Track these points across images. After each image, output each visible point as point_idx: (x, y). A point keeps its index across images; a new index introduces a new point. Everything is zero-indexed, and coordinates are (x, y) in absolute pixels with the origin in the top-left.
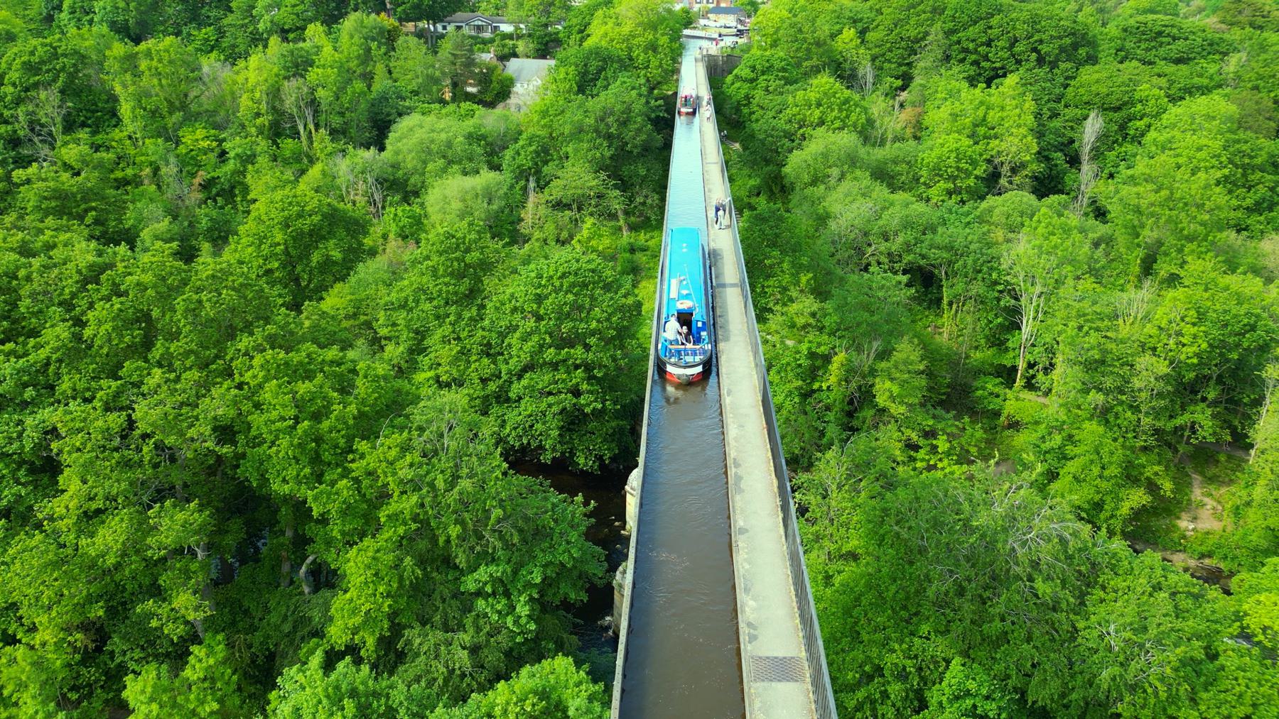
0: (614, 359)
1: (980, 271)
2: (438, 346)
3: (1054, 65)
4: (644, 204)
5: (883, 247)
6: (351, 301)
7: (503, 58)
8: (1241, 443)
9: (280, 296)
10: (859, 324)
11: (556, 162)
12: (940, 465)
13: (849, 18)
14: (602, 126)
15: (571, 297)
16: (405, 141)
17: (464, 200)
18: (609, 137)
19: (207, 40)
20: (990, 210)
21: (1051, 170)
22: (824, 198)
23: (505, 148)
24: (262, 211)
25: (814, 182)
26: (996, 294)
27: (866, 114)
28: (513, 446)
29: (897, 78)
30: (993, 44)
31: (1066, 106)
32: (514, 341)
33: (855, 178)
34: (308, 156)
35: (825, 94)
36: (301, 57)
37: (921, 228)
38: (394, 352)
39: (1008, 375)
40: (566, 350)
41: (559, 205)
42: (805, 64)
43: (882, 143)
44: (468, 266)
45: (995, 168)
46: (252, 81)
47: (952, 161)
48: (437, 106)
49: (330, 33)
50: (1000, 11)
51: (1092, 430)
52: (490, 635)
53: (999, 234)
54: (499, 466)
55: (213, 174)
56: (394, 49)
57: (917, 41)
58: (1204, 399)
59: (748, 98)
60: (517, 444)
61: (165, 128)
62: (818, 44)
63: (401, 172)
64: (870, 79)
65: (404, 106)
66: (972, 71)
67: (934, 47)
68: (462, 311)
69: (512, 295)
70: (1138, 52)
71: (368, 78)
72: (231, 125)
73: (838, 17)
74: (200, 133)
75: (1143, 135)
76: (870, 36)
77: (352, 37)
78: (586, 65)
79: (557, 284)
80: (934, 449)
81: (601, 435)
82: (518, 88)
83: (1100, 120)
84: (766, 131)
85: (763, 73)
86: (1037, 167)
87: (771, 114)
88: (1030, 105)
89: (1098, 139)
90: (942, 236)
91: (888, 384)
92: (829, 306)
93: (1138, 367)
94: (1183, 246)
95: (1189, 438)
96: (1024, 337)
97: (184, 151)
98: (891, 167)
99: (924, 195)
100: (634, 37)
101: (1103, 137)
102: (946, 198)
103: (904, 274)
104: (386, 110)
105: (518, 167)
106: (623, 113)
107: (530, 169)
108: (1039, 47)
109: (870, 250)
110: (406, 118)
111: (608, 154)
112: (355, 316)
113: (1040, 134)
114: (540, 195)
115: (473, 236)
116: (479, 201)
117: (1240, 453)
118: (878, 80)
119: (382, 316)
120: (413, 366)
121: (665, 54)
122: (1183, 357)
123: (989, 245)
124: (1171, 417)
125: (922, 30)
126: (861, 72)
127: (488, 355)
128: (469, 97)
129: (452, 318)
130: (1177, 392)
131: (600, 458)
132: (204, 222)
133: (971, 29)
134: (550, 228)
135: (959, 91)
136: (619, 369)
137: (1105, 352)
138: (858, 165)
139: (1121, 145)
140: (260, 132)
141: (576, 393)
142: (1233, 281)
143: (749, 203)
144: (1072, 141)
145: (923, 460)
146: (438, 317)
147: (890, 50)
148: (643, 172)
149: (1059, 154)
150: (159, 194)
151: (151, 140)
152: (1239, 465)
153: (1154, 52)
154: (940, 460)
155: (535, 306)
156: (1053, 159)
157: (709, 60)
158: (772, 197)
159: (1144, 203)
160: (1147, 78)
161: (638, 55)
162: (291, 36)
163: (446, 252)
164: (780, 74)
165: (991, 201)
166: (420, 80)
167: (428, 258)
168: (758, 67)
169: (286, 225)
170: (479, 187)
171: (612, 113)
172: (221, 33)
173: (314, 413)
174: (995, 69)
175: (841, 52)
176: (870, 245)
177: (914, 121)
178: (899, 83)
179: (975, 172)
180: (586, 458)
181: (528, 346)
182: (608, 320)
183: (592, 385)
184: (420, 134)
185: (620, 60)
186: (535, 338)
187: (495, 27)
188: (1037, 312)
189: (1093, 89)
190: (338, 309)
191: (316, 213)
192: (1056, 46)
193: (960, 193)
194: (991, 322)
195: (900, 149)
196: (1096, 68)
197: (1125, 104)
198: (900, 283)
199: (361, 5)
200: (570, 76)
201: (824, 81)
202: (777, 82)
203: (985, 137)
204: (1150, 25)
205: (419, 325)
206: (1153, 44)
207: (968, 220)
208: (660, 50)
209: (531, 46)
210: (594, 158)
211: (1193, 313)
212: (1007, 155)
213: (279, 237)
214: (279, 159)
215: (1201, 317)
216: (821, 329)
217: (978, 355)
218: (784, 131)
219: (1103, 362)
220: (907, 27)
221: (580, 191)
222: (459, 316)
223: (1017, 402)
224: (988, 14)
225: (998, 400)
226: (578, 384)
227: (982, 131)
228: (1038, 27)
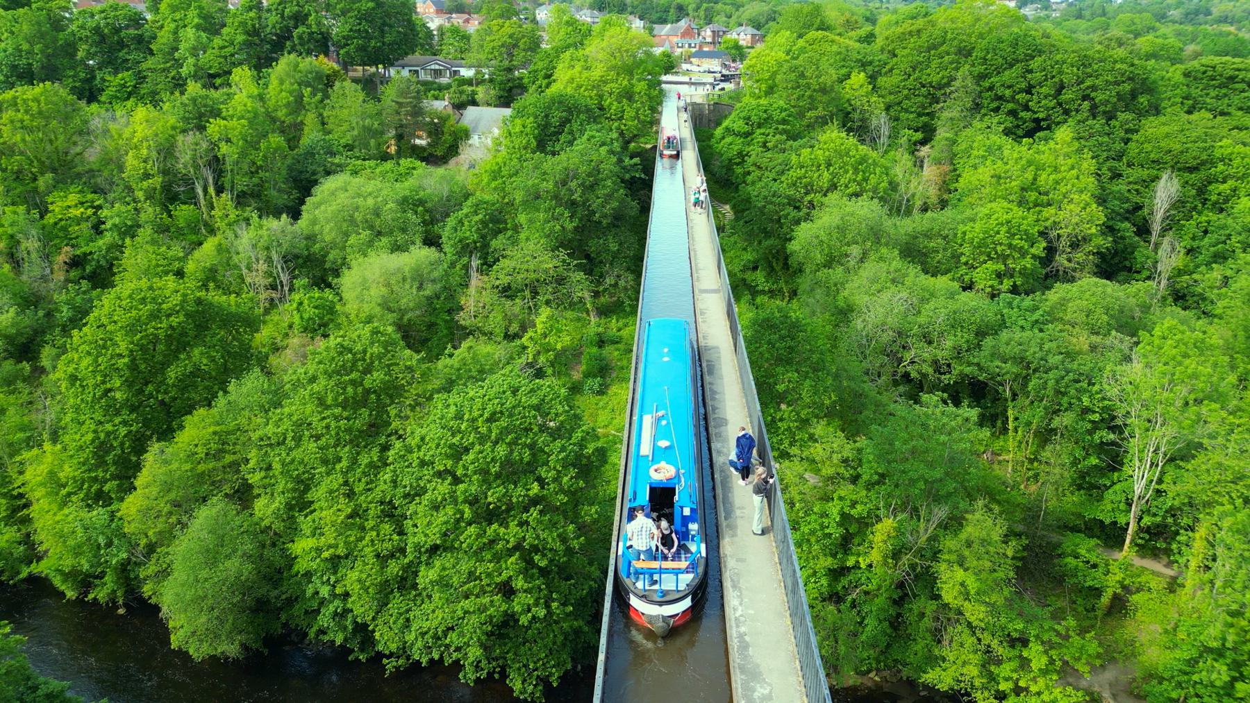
0: (563, 539)
1: (1064, 394)
2: (323, 504)
3: (1110, 116)
4: (616, 285)
5: (927, 353)
6: (215, 433)
7: (459, 107)
9: (125, 423)
10: (912, 482)
11: (509, 233)
12: (1033, 689)
13: (858, 61)
15: (502, 450)
16: (323, 207)
17: (388, 285)
19: (124, 86)
20: (1063, 303)
22: (842, 284)
23: (448, 215)
24: (106, 310)
25: (829, 263)
26: (1089, 426)
27: (887, 174)
28: (418, 663)
29: (916, 131)
30: (1034, 91)
31: (1129, 165)
32: (420, 509)
33: (881, 258)
34: (206, 225)
36: (205, 106)
37: (974, 327)
38: (266, 508)
40: (495, 526)
41: (507, 292)
42: (809, 114)
43: (908, 212)
44: (368, 392)
46: (139, 135)
47: (1002, 237)
48: (372, 163)
49: (260, 78)
50: (1040, 52)
53: (1082, 340)
55: (85, 249)
56: (328, 97)
57: (940, 87)
59: (742, 156)
60: (424, 661)
61: (35, 190)
62: (823, 90)
63: (317, 246)
64: (885, 131)
65: (333, 164)
66: (1009, 122)
67: (961, 93)
68: (358, 454)
70: (1208, 100)
71: (292, 133)
72: (115, 188)
73: (844, 60)
74: (73, 198)
75: (1226, 201)
76: (882, 81)
77: (282, 82)
78: (547, 116)
80: (1024, 664)
81: (545, 646)
82: (475, 140)
83: (1176, 181)
84: (765, 198)
85: (759, 126)
86: (1105, 243)
87: (772, 175)
88: (1089, 164)
89: (1173, 206)
90: (1008, 341)
91: (960, 574)
92: (862, 441)
97: (52, 221)
98: (923, 243)
99: (967, 278)
100: (605, 82)
101: (1179, 204)
102: (995, 283)
104: (311, 168)
105: (460, 241)
106: (589, 175)
107: (475, 242)
108: (1093, 95)
109: (908, 356)
110: (331, 178)
111: (570, 226)
112: (218, 455)
113: (1102, 200)
114: (486, 278)
115: (376, 349)
116: (407, 286)
118: (894, 136)
119: (253, 455)
120: (293, 530)
121: (642, 103)
123: (1070, 355)
125: (946, 73)
126: (874, 122)
127: (391, 516)
128: (417, 153)
131: (544, 681)
132: (65, 310)
133: (1007, 73)
134: (495, 321)
135: (1000, 148)
136: (569, 551)
138: (883, 241)
139: (1200, 213)
140: (149, 197)
141: (507, 591)
143: (744, 280)
144: (1139, 207)
145: (1007, 679)
146: (325, 462)
147: (907, 98)
148: (614, 247)
149: (1127, 225)
150: (12, 275)
151: (11, 208)
153: (1226, 101)
154: (1034, 679)
155: (449, 463)
156: (1119, 230)
157: (693, 109)
158: (771, 272)
160: (1224, 132)
161: (611, 104)
162: (218, 81)
163: (338, 373)
164: (781, 127)
165: (1059, 292)
166: (356, 133)
167: (313, 379)
168: (754, 118)
169: (131, 329)
170: (407, 269)
171: (575, 177)
172: (141, 78)
174: (1037, 121)
175: (848, 100)
177: (940, 182)
179: (1033, 251)
180: (524, 681)
181: (440, 518)
182: (555, 480)
184: (343, 198)
185: (588, 110)
186: (450, 510)
187: (455, 72)
189: (1162, 145)
190: (196, 446)
191: (178, 312)
192: (1114, 93)
193: (1012, 276)
195: (934, 219)
196: (1162, 119)
197: (1203, 163)
198: (967, 420)
199: (298, 47)
200: (528, 130)
201: (833, 136)
202: (778, 136)
203: (1036, 205)
204: (1219, 68)
205: (301, 469)
206: (1224, 91)
207: (1036, 316)
208: (637, 97)
210: (552, 230)
212: (1066, 227)
213: (123, 346)
214: (173, 230)
216: (855, 479)
218: (788, 197)
220: (928, 71)
221: (533, 276)
222: (354, 462)
224: (1026, 55)
225: (1099, 573)
227: (1032, 196)
228: (1089, 70)
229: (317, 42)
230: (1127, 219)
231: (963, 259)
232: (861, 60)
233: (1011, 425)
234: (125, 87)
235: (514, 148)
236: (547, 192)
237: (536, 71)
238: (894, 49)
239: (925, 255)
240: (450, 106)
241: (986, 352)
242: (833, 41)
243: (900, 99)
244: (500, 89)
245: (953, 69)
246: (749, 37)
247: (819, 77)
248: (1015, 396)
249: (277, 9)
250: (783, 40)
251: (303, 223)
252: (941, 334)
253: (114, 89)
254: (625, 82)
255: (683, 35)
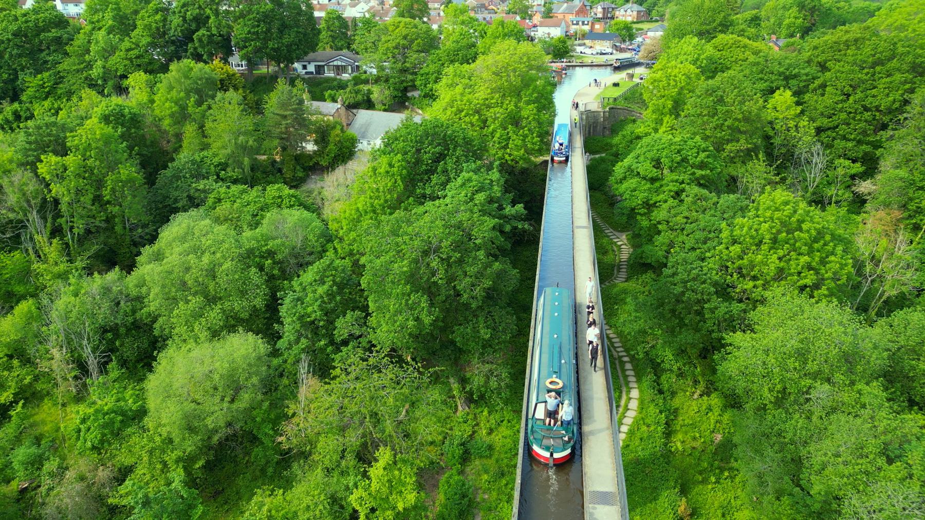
18: (431, 291)
29: (854, 161)
35: (783, 224)
42: (728, 147)
63: (145, 310)
73: (761, 72)
77: (171, 88)
78: (418, 151)
84: (685, 282)
100: (489, 107)
138: (859, 368)
157: (587, 117)
161: (494, 131)
164: (699, 173)
166: (229, 151)
175: (771, 123)
178: (858, 168)
208: (524, 123)
209: (387, 92)
220: (874, 92)
229: (218, 43)
232: (783, 73)
234: (44, 87)
235: (378, 190)
237: (427, 74)
238: (826, 61)
240: (343, 109)
242: (745, 46)
243: (836, 123)
244: (395, 89)
245: (906, 91)
246: (635, 13)
247: (742, 103)
249: (180, 12)
250: (690, 48)
251: (132, 280)
253: (32, 90)
254: (511, 107)
255: (578, 13)
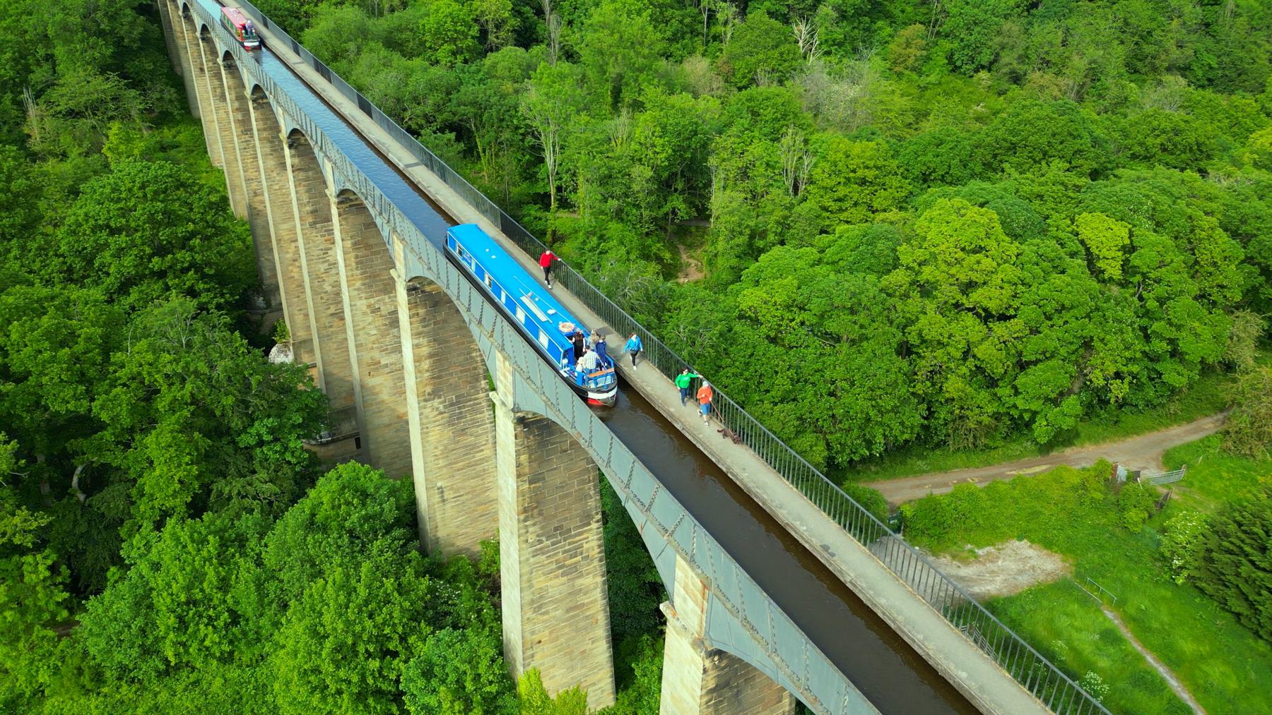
1: (502, 120)
4: (161, 99)
5: (419, 110)
8: (703, 214)
14: (89, 24)
18: (101, 34)
20: (494, 66)
21: (524, 22)
22: (349, 72)
26: (521, 137)
39: (543, 200)
43: (381, 14)
44: (17, 195)
45: (482, 26)
47: (449, 25)
51: (614, 227)
52: (276, 471)
53: (508, 87)
54: (242, 345)
58: (676, 190)
69: (86, 215)
79: (140, 194)
86: (515, 22)
93: (633, 175)
94: (637, 76)
95: (673, 219)
96: (550, 168)
99: (433, 58)
102: (452, 59)
103: (451, 132)
109: (407, 115)
111: (109, 52)
117: (702, 224)
122: (659, 162)
123: (503, 97)
124: (659, 207)
127: (72, 280)
129: (15, 252)
130: (659, 189)
137: (610, 168)
142: (674, 100)
149: (528, 8)
152: (705, 232)
159: (605, 46)
165: (491, 58)
171: (96, 9)
173: (61, 341)
176: (405, 110)
179: (471, 33)
182: (201, 219)
183: (206, 283)
188: (554, 147)
193: (462, 53)
194: (520, 160)
195: (400, 17)
198: (449, 140)
207: (480, 75)
211: (658, 129)
215: (664, 128)
217: (515, 191)
218: (287, 10)
219: (610, 177)
222: (23, 248)
223: (558, 220)
225: (542, 222)
226: (193, 285)
230: (528, 4)
231: (428, 45)
233: (482, 154)
236: (76, 25)
239: (401, 45)
241: (454, 102)
248: (478, 130)
252: (425, 97)
